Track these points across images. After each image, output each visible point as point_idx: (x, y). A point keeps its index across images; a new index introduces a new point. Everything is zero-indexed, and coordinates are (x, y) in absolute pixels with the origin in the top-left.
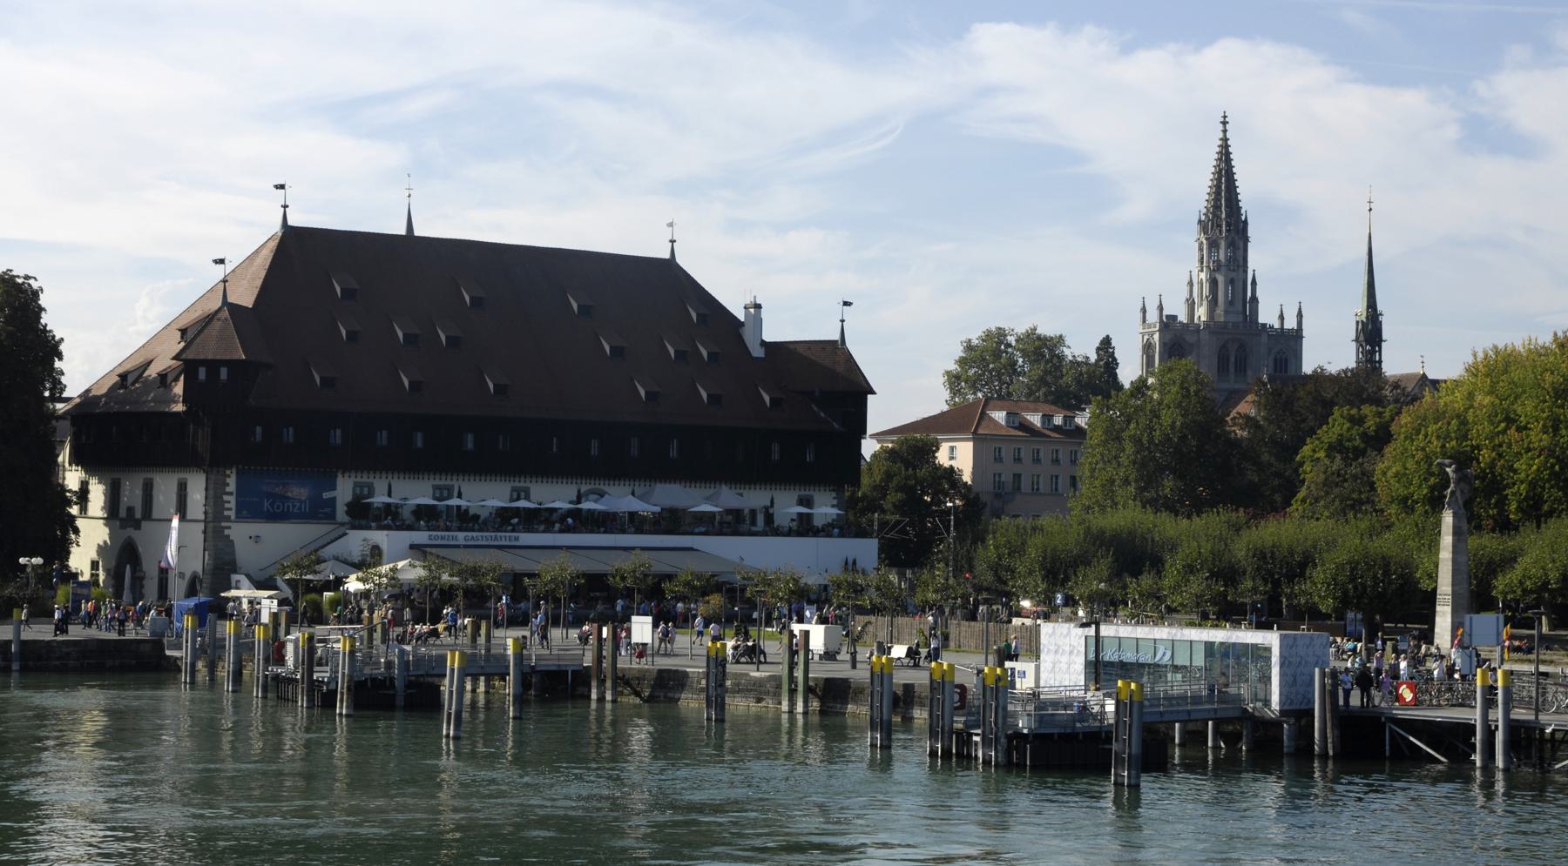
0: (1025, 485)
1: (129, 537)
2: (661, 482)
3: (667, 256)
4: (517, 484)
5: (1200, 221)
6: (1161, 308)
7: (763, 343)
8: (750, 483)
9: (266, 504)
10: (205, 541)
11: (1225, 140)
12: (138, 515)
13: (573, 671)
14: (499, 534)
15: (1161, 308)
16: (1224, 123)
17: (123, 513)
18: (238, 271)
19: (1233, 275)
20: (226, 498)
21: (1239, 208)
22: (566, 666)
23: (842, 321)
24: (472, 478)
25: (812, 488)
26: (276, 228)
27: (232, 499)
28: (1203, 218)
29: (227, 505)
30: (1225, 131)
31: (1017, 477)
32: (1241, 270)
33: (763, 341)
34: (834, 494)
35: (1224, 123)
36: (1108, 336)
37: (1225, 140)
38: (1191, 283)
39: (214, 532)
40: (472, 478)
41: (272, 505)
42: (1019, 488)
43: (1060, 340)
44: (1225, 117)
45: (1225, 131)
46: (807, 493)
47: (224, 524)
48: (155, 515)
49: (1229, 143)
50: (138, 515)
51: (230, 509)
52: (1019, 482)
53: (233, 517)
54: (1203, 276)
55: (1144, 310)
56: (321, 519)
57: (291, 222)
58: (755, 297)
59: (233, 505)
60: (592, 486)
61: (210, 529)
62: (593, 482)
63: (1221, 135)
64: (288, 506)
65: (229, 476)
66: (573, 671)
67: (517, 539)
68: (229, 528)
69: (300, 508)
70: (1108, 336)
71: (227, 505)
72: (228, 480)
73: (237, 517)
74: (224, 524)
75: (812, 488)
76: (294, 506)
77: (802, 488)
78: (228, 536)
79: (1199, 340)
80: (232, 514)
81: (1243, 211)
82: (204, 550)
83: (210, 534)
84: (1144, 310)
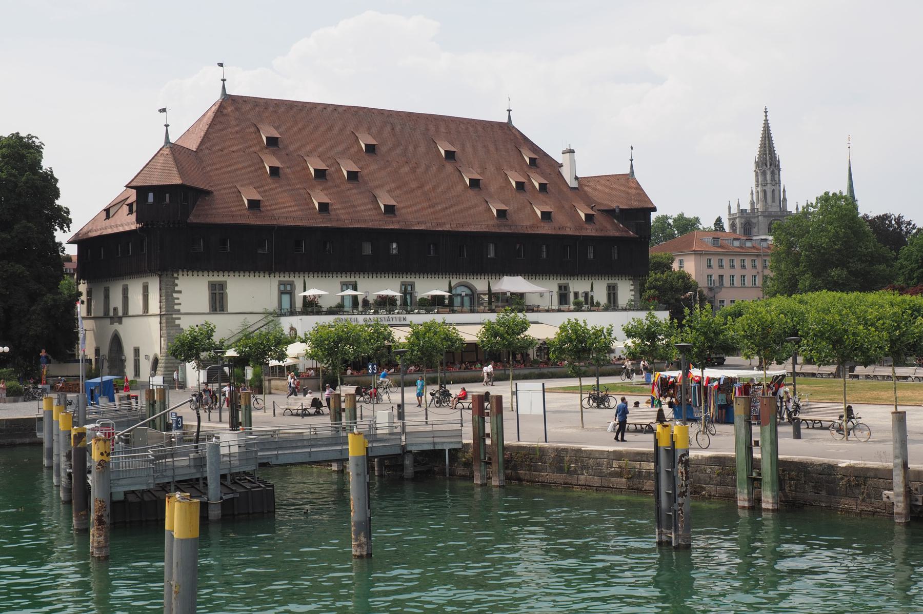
0: (726, 281)
2: (507, 276)
3: (506, 121)
4: (405, 280)
5: (756, 162)
6: (739, 206)
7: (576, 178)
8: (574, 276)
10: (161, 330)
11: (766, 120)
13: (450, 450)
14: (391, 316)
15: (739, 206)
16: (766, 112)
17: (111, 314)
18: (191, 130)
19: (773, 187)
21: (775, 154)
22: (443, 443)
23: (631, 160)
24: (366, 276)
25: (617, 278)
26: (217, 97)
28: (757, 160)
30: (766, 116)
31: (721, 277)
32: (778, 185)
33: (576, 177)
34: (631, 282)
35: (766, 112)
36: (720, 217)
37: (766, 120)
38: (752, 194)
39: (167, 322)
40: (366, 276)
42: (722, 284)
43: (697, 220)
44: (766, 109)
45: (766, 116)
46: (613, 281)
47: (174, 316)
48: (130, 313)
49: (769, 122)
50: (120, 314)
52: (722, 280)
54: (759, 189)
55: (730, 208)
57: (229, 92)
58: (569, 145)
60: (461, 280)
61: (164, 321)
62: (461, 277)
63: (764, 118)
66: (450, 450)
67: (405, 319)
68: (179, 319)
70: (720, 217)
74: (174, 316)
75: (617, 278)
77: (610, 278)
78: (179, 325)
79: (758, 221)
81: (777, 156)
82: (161, 337)
83: (164, 325)
84: (730, 208)
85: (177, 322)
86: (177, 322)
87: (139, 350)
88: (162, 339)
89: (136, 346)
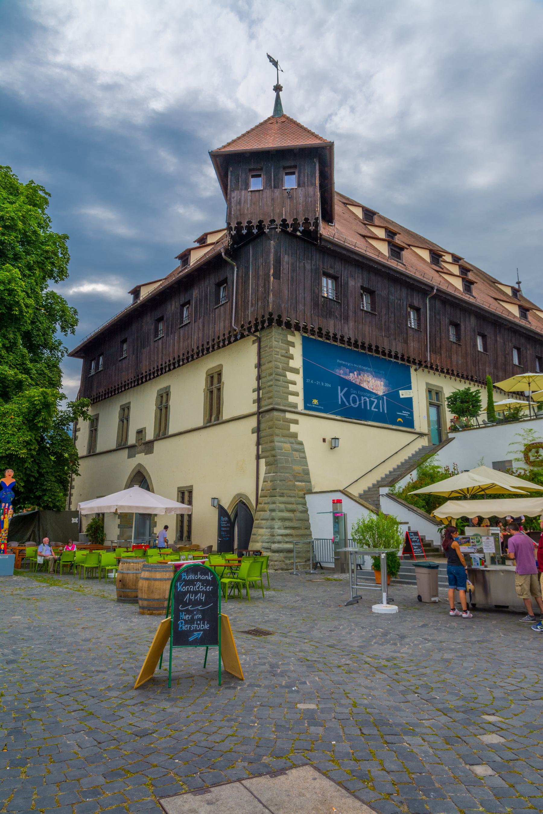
1: (139, 465)
9: (340, 395)
10: (258, 444)
12: (150, 435)
17: (132, 440)
20: (290, 376)
27: (299, 379)
29: (292, 388)
41: (347, 395)
51: (296, 394)
53: (301, 407)
56: (400, 424)
59: (299, 387)
64: (365, 403)
65: (293, 345)
68: (296, 422)
69: (377, 406)
71: (292, 388)
72: (292, 350)
73: (306, 408)
74: (289, 416)
76: (371, 403)
78: (295, 435)
80: (299, 401)
82: (258, 457)
85: (293, 428)
86: (293, 428)
87: (190, 492)
88: (263, 462)
89: (184, 484)
